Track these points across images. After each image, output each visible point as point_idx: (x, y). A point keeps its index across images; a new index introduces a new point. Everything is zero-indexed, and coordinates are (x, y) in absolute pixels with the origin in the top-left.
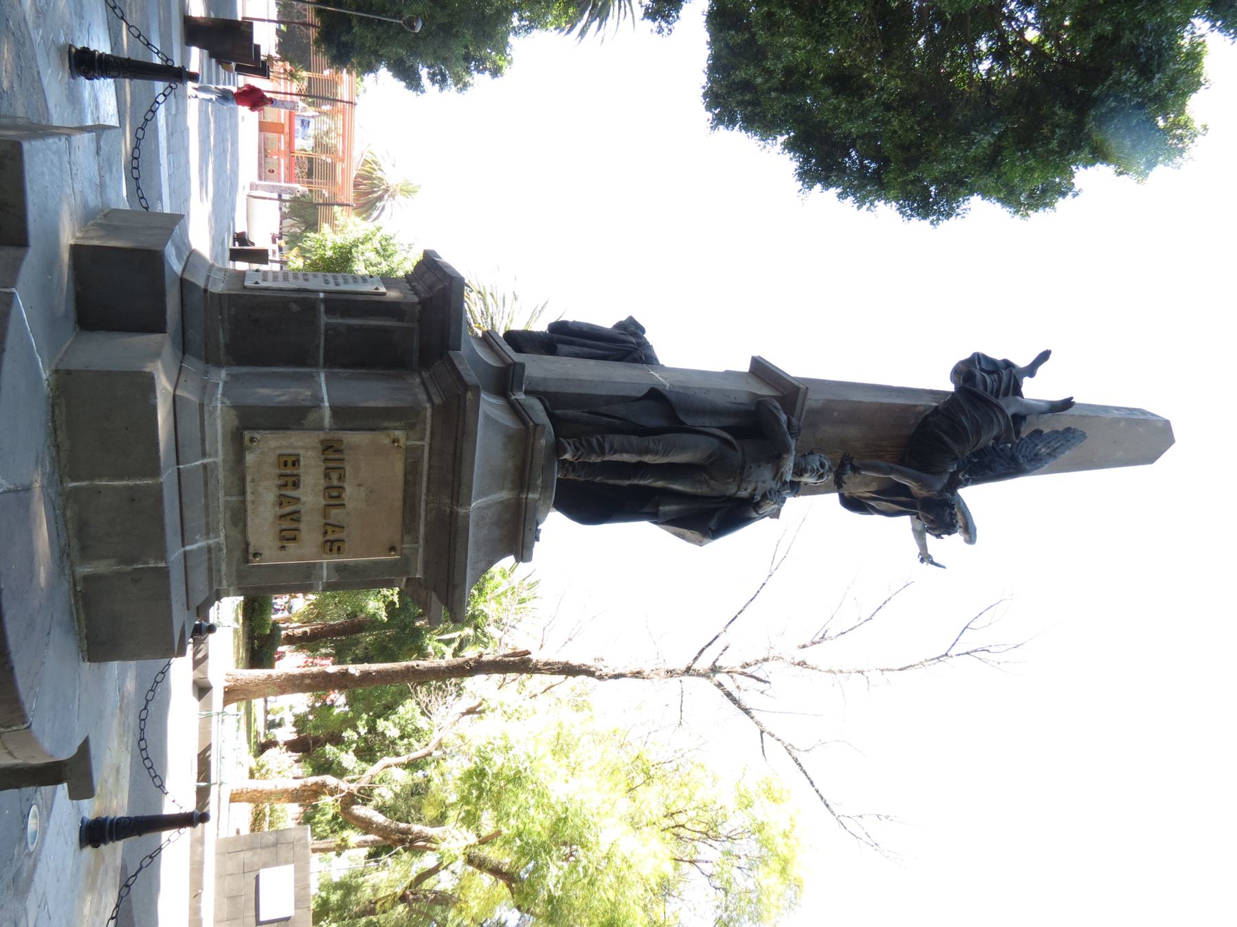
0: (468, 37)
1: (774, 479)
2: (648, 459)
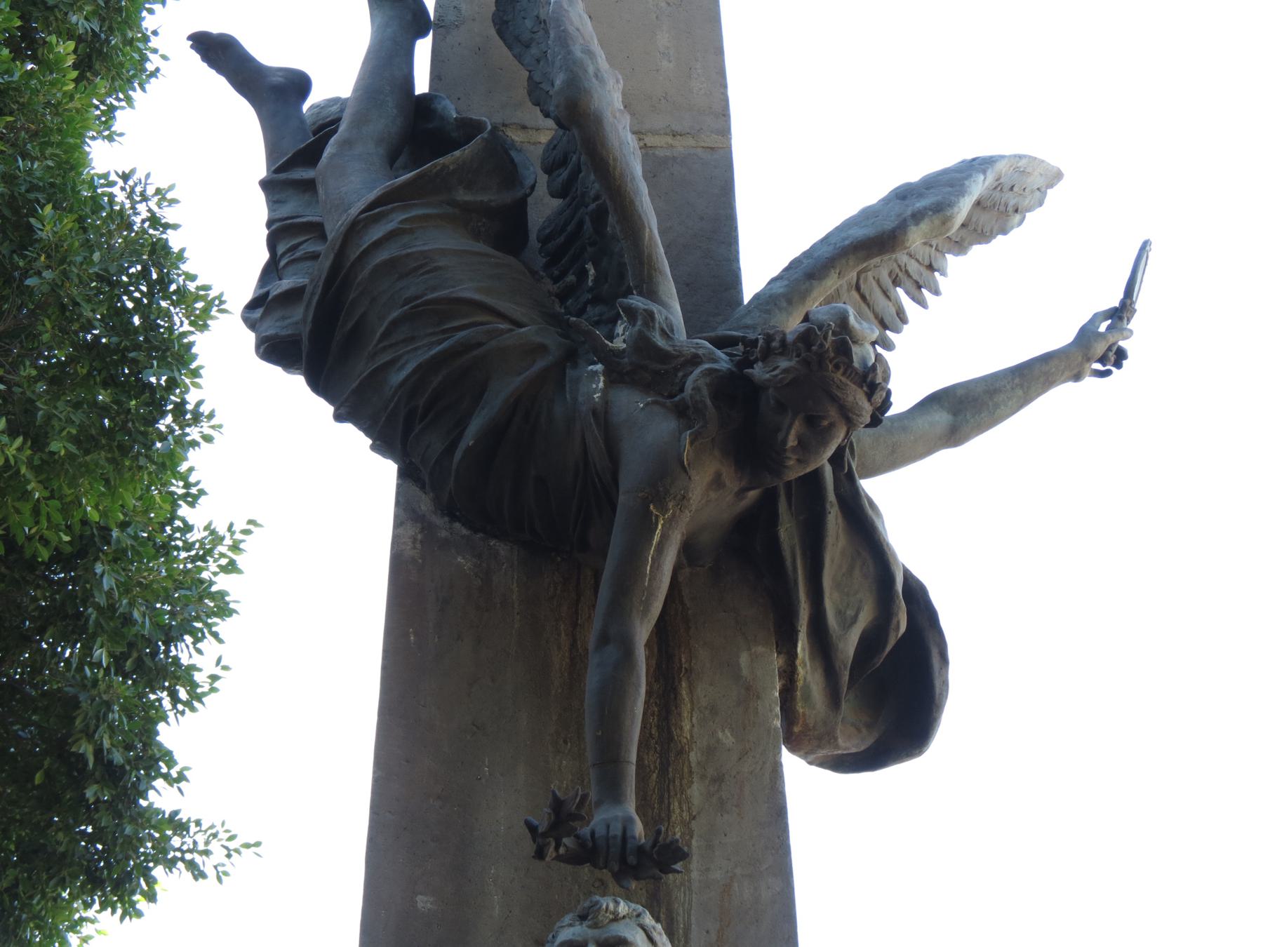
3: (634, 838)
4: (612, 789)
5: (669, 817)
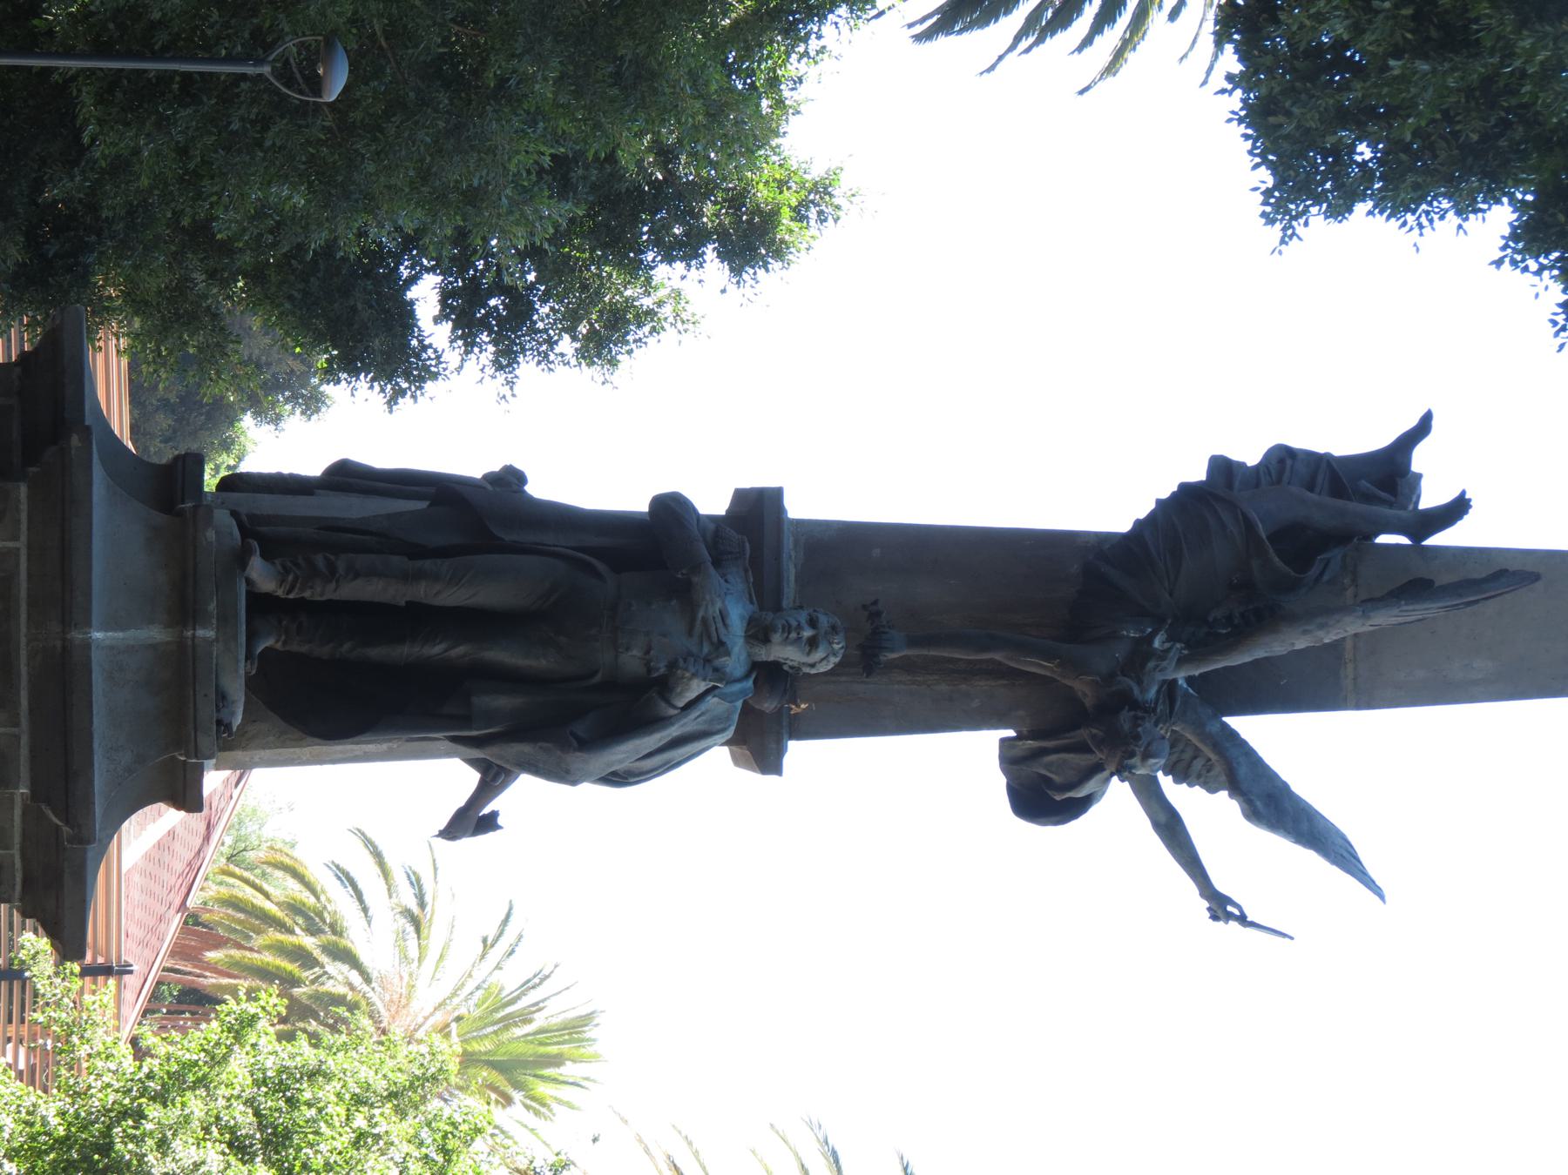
0: (544, 90)
1: (690, 633)
2: (422, 592)
4: (913, 642)
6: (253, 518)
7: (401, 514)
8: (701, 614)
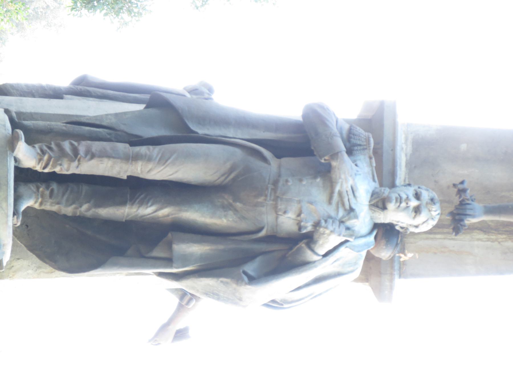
3: (466, 218)
4: (490, 211)
5: (500, 234)
6: (19, 114)
7: (125, 113)
8: (337, 188)
